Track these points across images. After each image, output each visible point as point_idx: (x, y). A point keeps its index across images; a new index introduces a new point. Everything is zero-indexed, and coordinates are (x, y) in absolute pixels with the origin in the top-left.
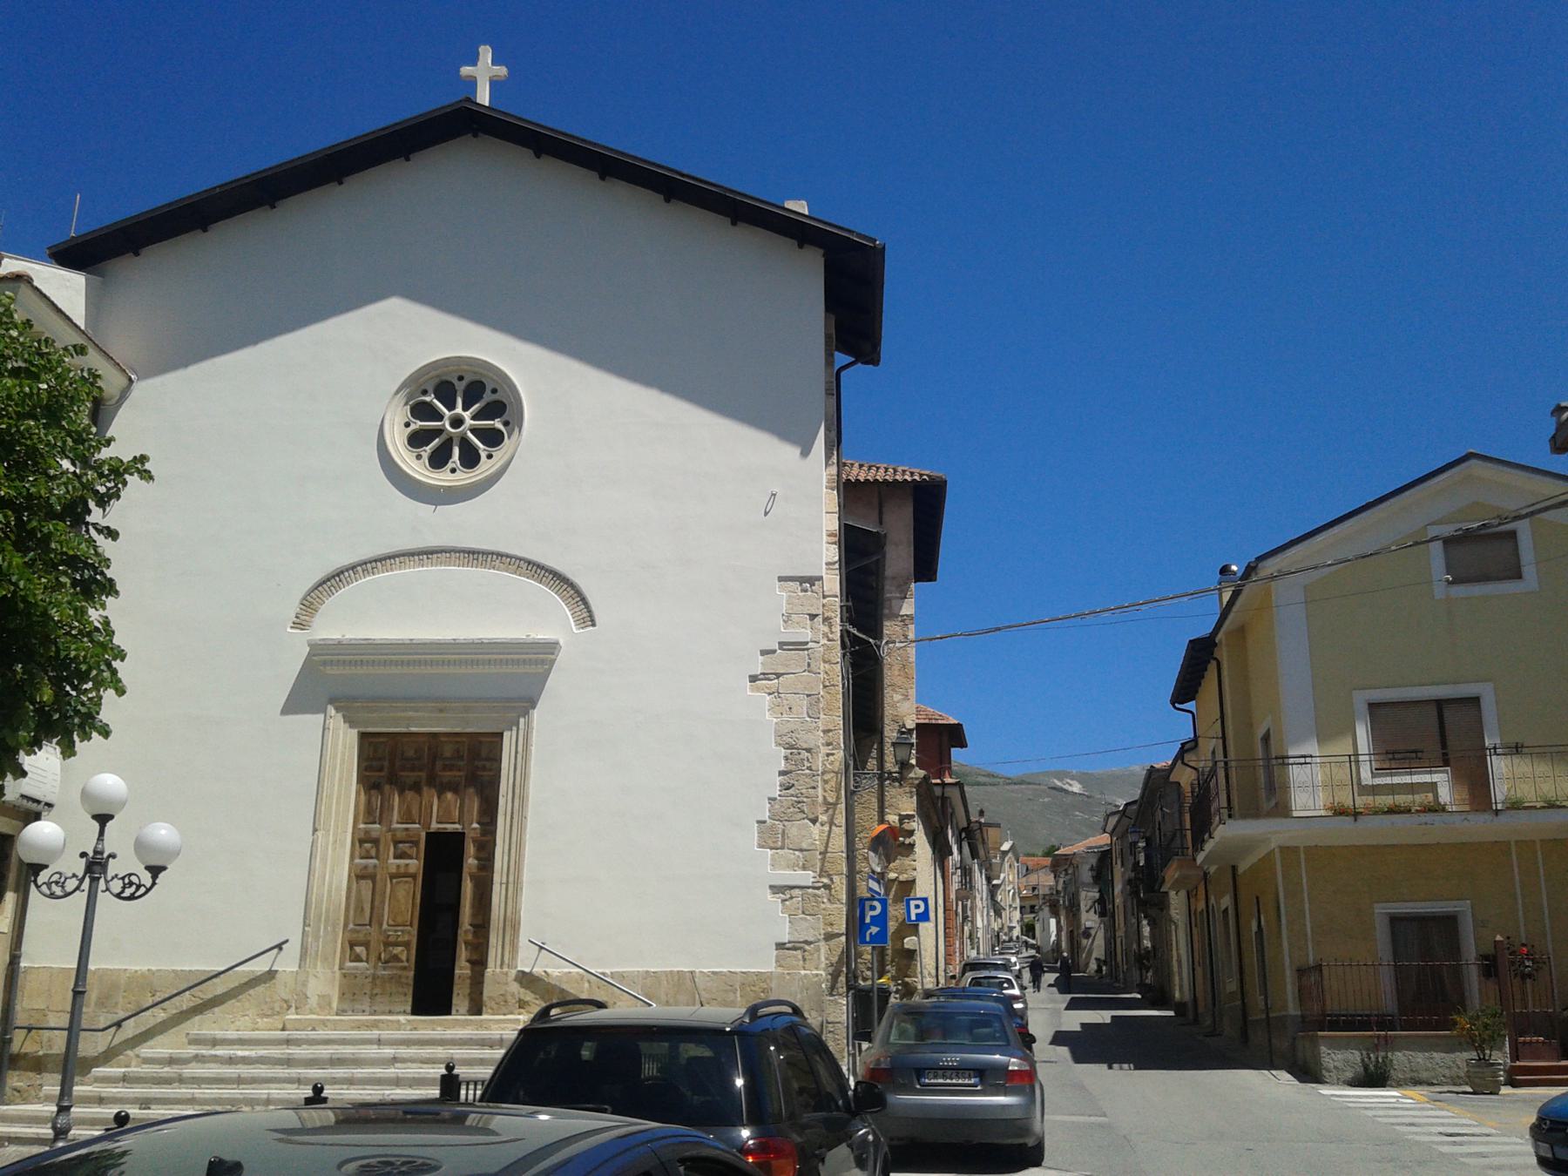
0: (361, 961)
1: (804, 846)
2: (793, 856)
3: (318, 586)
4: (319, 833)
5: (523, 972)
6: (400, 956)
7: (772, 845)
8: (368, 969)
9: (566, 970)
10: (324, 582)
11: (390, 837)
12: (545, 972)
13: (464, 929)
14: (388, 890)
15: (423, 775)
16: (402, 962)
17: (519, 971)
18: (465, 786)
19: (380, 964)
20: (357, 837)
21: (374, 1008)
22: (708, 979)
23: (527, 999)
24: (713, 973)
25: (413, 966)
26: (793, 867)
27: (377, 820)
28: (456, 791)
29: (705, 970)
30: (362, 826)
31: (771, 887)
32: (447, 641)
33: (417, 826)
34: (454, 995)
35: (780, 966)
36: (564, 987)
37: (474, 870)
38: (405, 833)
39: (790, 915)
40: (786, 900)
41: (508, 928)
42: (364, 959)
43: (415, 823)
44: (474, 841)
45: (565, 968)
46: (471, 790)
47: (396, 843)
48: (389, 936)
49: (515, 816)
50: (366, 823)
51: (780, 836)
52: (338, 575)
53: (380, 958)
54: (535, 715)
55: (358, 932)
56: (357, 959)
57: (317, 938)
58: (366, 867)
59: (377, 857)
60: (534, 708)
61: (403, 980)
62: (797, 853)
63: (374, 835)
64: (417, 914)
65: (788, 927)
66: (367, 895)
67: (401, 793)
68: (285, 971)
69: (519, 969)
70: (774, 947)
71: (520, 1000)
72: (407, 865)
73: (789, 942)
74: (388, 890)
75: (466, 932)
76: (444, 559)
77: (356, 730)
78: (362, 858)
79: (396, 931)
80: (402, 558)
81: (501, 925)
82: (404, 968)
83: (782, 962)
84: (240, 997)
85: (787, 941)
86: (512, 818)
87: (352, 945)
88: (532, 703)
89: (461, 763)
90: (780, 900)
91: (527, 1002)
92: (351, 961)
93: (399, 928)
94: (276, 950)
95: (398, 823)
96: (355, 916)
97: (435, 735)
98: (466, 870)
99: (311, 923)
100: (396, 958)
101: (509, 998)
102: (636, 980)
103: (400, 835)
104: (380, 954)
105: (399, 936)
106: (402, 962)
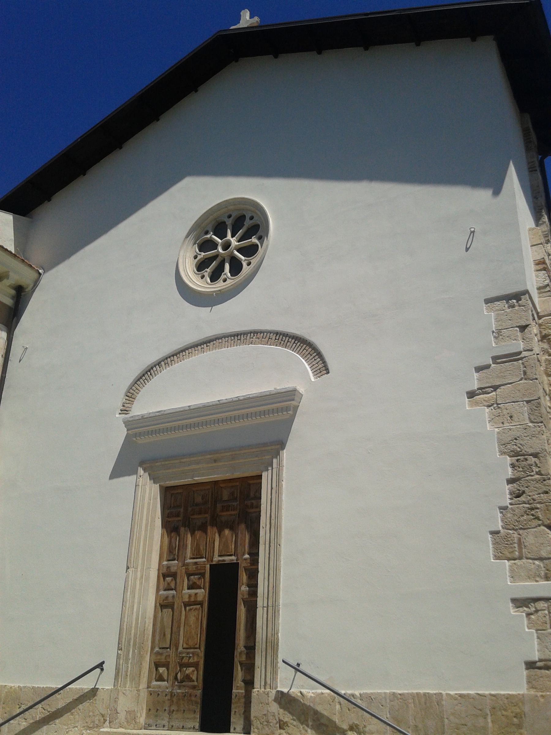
0: (164, 681)
1: (544, 554)
2: (533, 566)
3: (137, 381)
4: (130, 571)
5: (282, 692)
6: (191, 676)
7: (509, 555)
8: (167, 688)
9: (319, 691)
10: (141, 378)
11: (184, 570)
12: (301, 693)
13: (239, 650)
14: (183, 617)
15: (208, 516)
16: (193, 681)
17: (278, 691)
18: (238, 523)
19: (176, 683)
20: (161, 572)
21: (171, 724)
22: (456, 702)
23: (286, 720)
24: (461, 696)
25: (201, 685)
26: (534, 577)
27: (176, 557)
28: (232, 528)
29: (452, 693)
30: (165, 563)
31: (514, 600)
32: (214, 403)
33: (204, 560)
34: (232, 713)
35: (532, 688)
36: (319, 708)
37: (246, 596)
38: (194, 567)
39: (537, 630)
40: (531, 614)
41: (269, 651)
42: (166, 678)
43: (202, 558)
44: (246, 570)
45: (317, 689)
46: (243, 526)
47: (189, 575)
48: (183, 658)
49: (272, 545)
50: (169, 560)
51: (516, 545)
52: (149, 371)
53: (176, 678)
54: (285, 454)
55: (161, 654)
56: (160, 678)
57: (127, 660)
58: (167, 598)
59: (175, 589)
60: (283, 448)
61: (193, 698)
62: (537, 562)
63: (173, 569)
64: (204, 638)
65: (536, 643)
66: (168, 621)
67: (193, 534)
68: (103, 689)
69: (279, 689)
70: (524, 666)
71: (280, 721)
72: (196, 594)
73: (540, 660)
74: (183, 617)
75: (241, 653)
76: (218, 344)
77: (158, 485)
78: (165, 590)
79: (188, 653)
80: (190, 350)
81: (264, 646)
82: (194, 687)
83: (534, 682)
84: (73, 711)
85: (537, 659)
86: (270, 546)
87: (157, 665)
88: (282, 445)
89: (235, 504)
90: (524, 614)
91: (286, 722)
92: (157, 681)
93: (192, 650)
94: (98, 670)
95: (191, 558)
96: (159, 641)
97: (216, 483)
98: (240, 597)
99: (123, 647)
100: (188, 678)
101: (271, 718)
102: (384, 703)
103: (192, 568)
104: (177, 674)
105: (190, 657)
106: (193, 681)
